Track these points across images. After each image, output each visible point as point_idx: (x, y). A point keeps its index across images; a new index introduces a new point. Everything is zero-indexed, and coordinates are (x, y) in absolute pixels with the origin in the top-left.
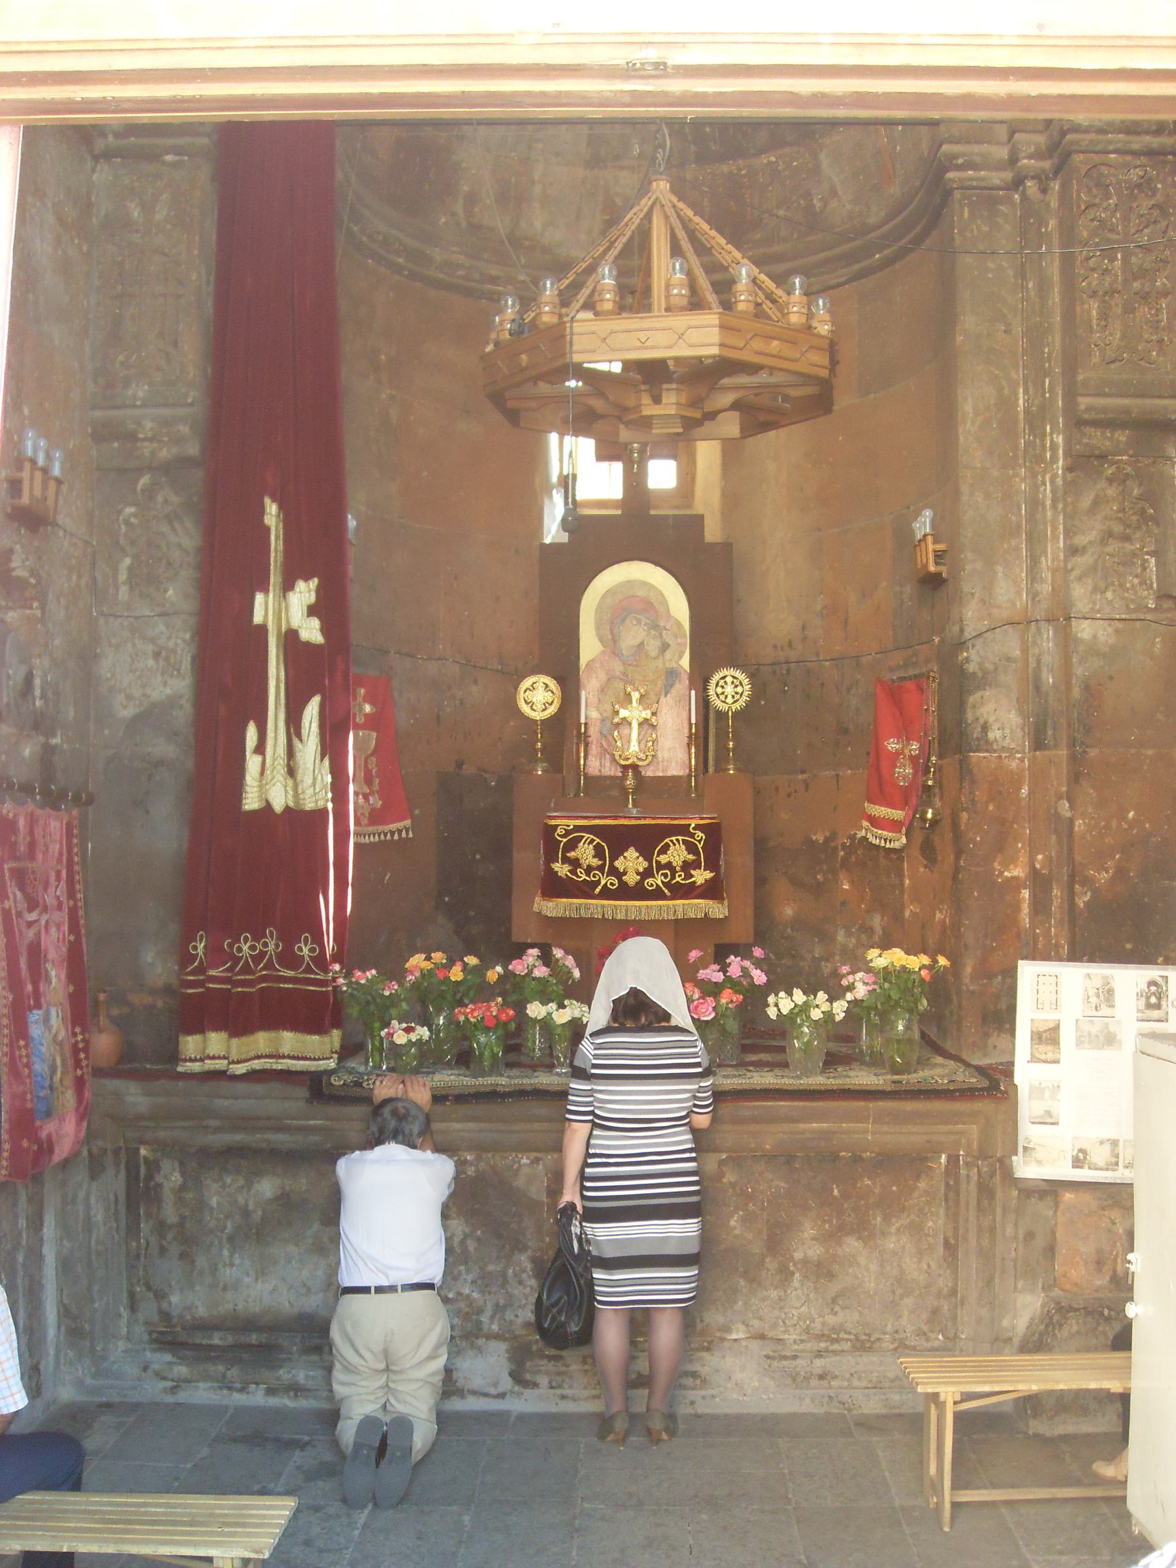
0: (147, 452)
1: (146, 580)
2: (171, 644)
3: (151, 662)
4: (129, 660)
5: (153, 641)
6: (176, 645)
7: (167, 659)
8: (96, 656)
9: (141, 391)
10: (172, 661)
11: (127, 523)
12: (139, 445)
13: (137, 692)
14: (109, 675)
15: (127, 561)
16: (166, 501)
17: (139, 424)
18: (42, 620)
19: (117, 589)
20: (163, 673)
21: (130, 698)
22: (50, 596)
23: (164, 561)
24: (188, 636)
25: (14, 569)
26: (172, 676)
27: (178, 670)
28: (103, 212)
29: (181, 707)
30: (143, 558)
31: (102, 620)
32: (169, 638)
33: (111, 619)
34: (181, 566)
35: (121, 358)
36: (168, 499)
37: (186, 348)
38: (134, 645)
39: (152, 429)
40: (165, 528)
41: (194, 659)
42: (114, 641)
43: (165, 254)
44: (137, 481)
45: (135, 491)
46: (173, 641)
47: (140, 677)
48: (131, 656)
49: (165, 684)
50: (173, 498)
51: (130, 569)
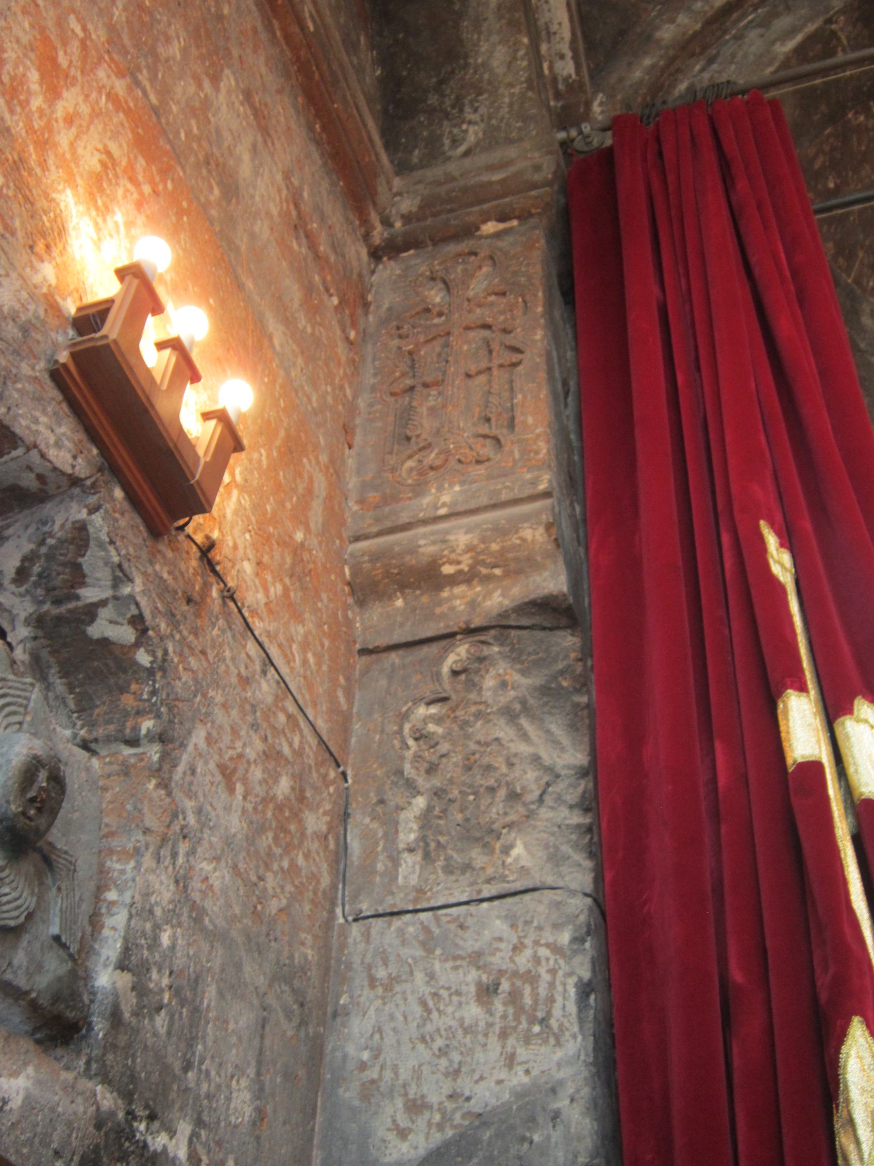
0: (459, 604)
1: (462, 830)
2: (523, 961)
3: (473, 1011)
4: (418, 1010)
5: (476, 959)
6: (537, 960)
7: (514, 997)
8: (335, 1015)
9: (446, 496)
10: (528, 1001)
11: (420, 736)
12: (445, 594)
13: (435, 1092)
14: (366, 1056)
15: (420, 802)
16: (504, 685)
17: (444, 541)
18: (162, 771)
19: (395, 861)
20: (504, 1035)
21: (415, 1107)
22: (199, 737)
23: (502, 793)
24: (565, 937)
25: (91, 612)
26: (527, 1039)
27: (544, 1021)
28: (387, 306)
29: (556, 1116)
30: (455, 793)
31: (356, 930)
32: (517, 948)
33: (378, 925)
34: (541, 800)
35: (410, 464)
36: (504, 679)
37: (530, 420)
38: (431, 976)
39: (470, 549)
40: (503, 731)
41: (585, 990)
42: (381, 973)
43: (487, 327)
44: (441, 659)
45: (438, 674)
46: (528, 952)
47: (443, 1052)
48: (423, 1003)
49: (510, 1061)
50: (524, 683)
51: (426, 819)
